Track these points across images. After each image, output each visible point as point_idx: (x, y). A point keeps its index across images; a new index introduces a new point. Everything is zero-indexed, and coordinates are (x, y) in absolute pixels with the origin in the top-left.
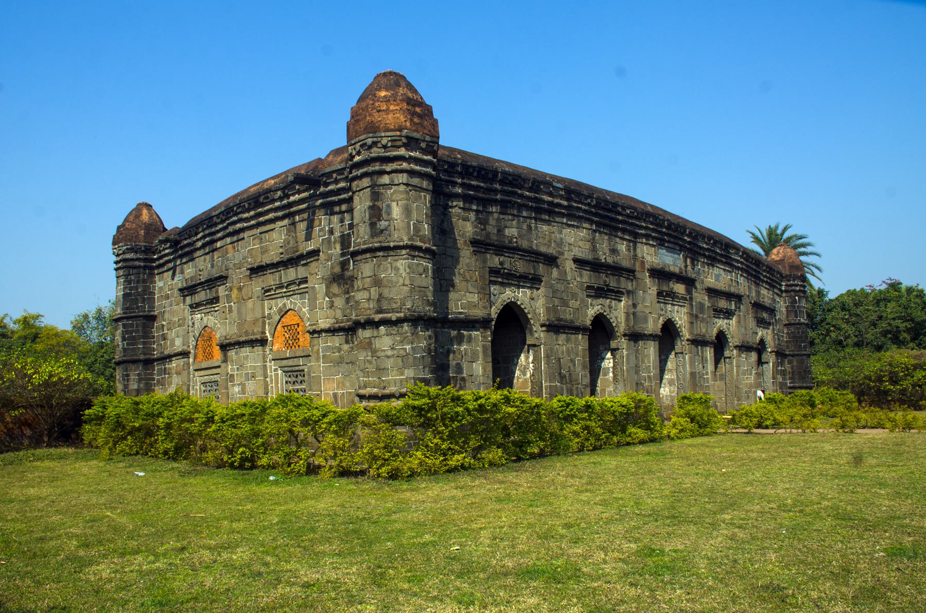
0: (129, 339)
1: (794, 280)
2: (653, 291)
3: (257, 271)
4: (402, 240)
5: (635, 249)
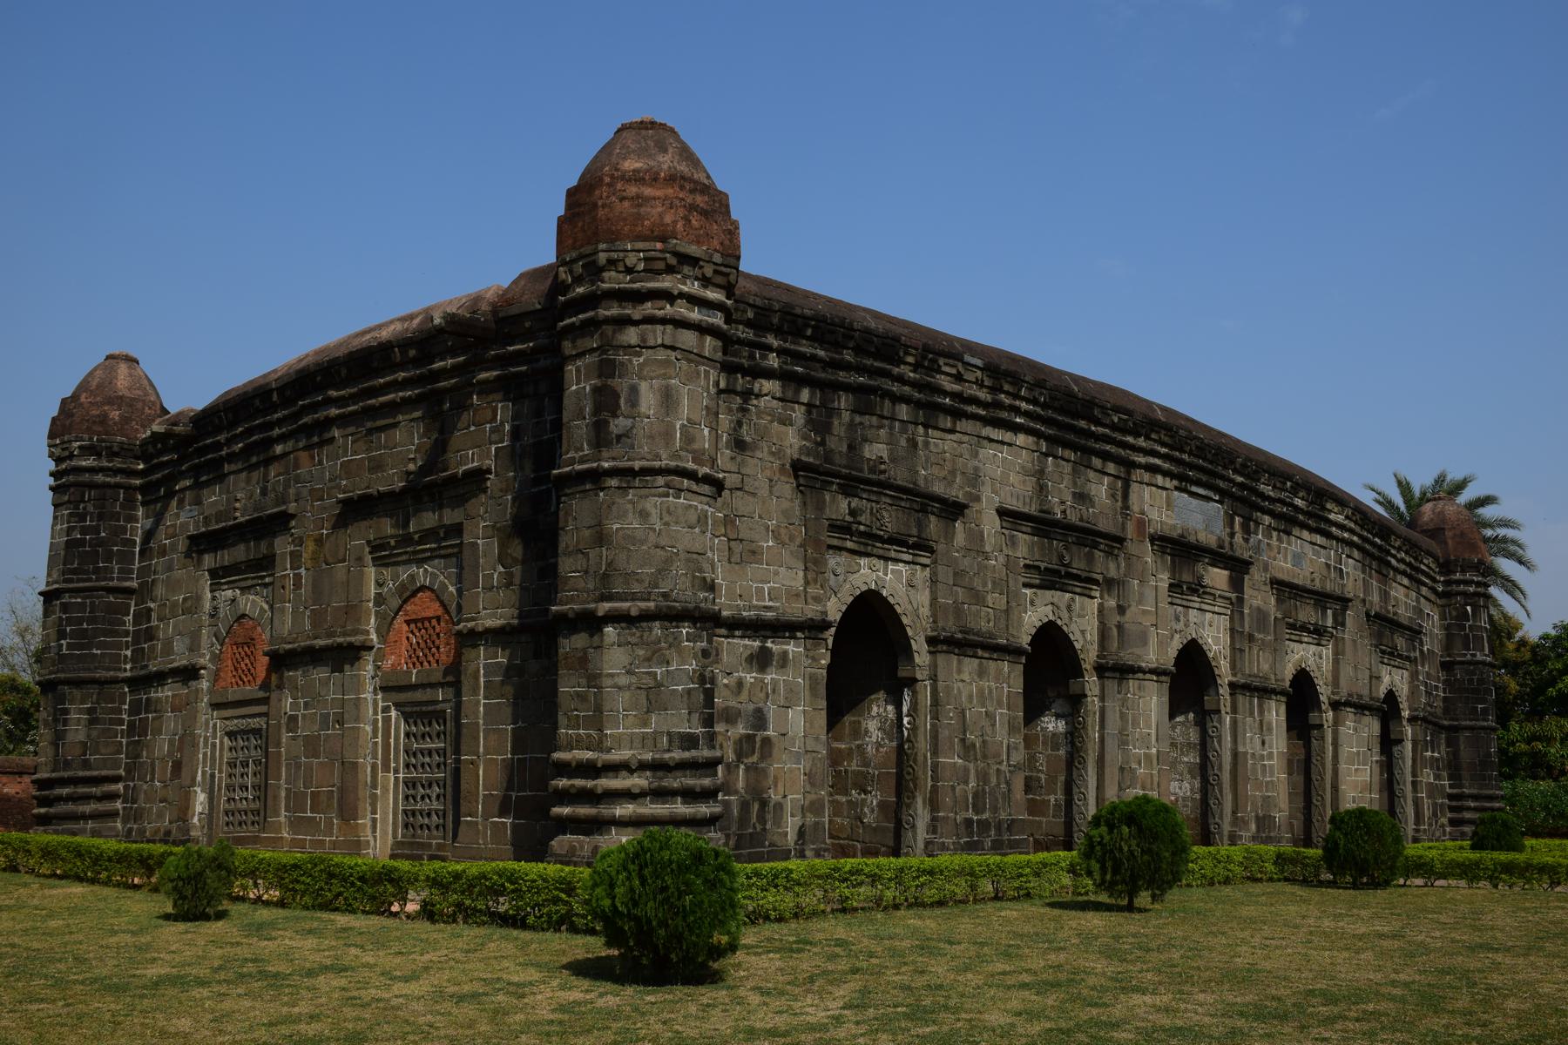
0: (73, 634)
1: (1463, 572)
2: (1164, 580)
3: (355, 509)
4: (658, 457)
5: (1126, 496)
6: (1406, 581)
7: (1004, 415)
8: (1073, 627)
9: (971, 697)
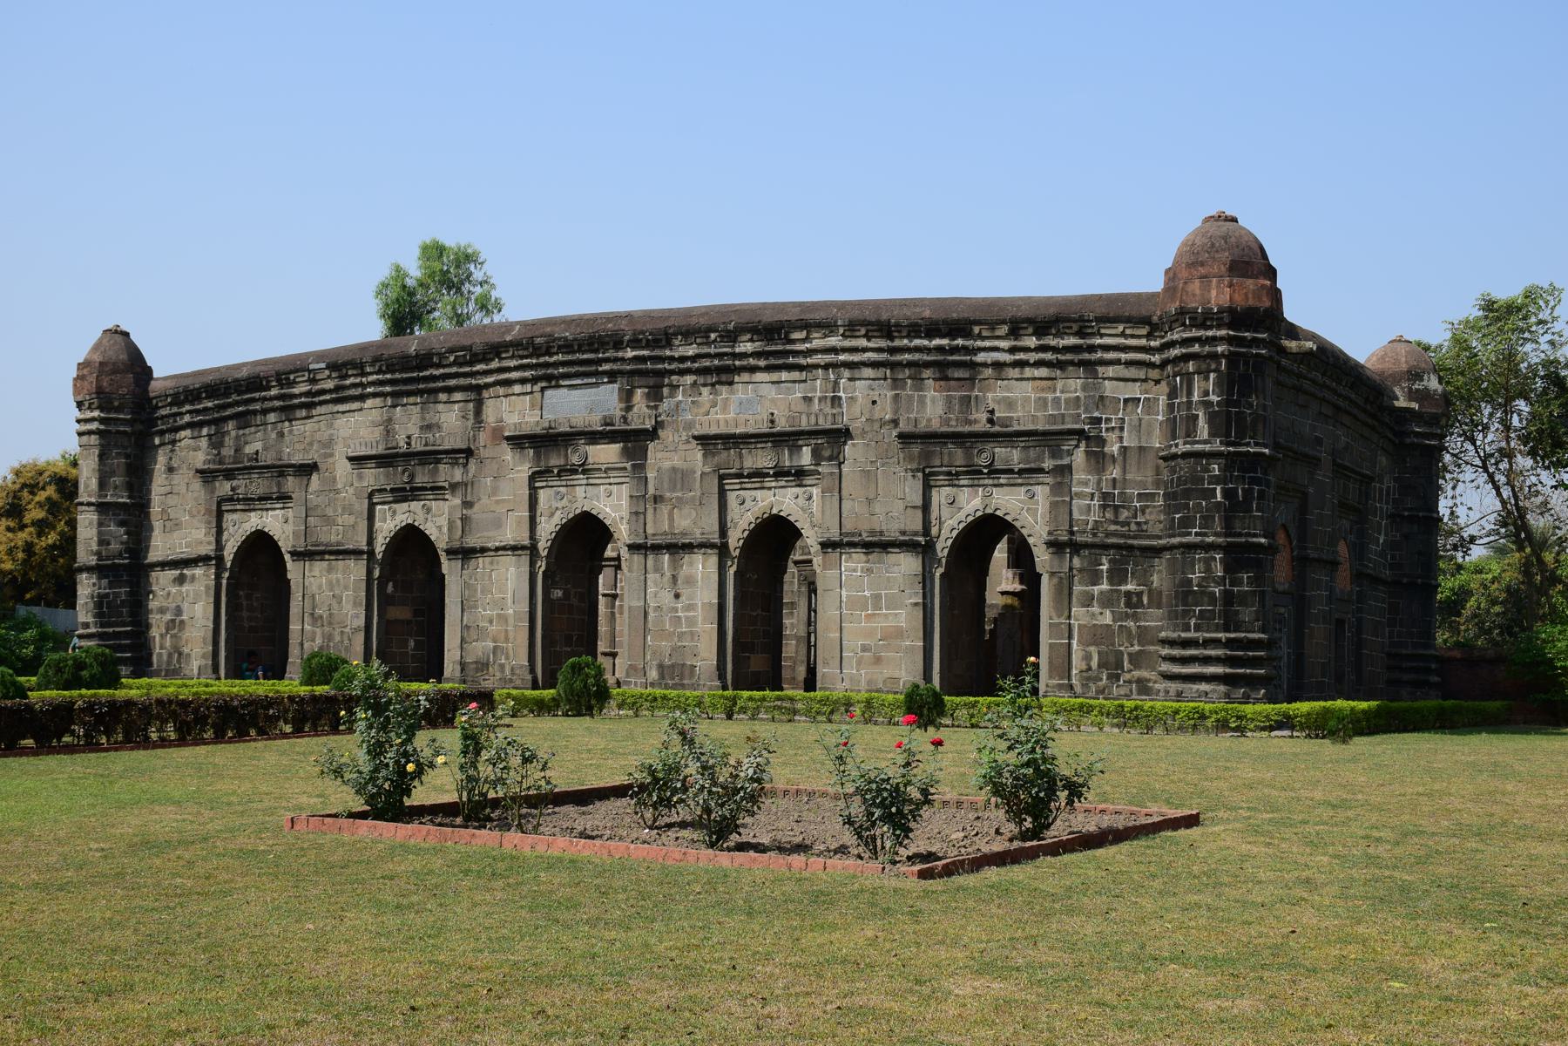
5: (478, 412)
6: (1043, 372)
7: (352, 392)
8: (429, 524)
9: (320, 587)
